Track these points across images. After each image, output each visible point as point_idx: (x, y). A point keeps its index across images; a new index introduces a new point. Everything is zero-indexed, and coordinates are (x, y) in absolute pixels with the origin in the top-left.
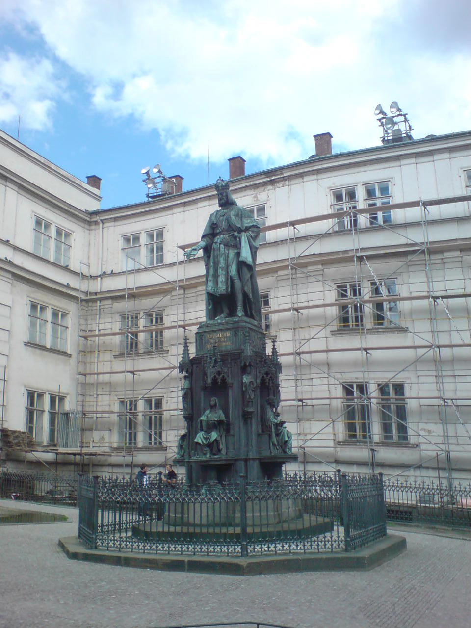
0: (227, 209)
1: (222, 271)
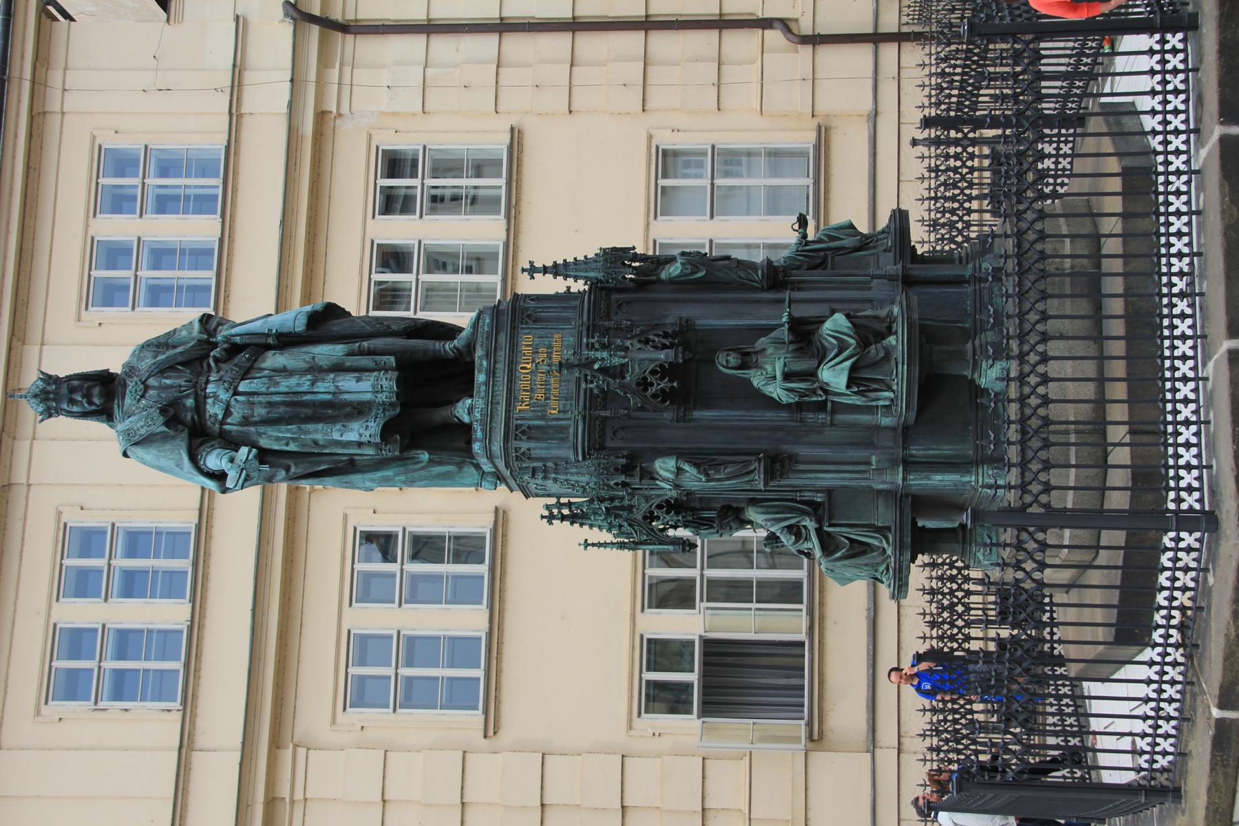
0: (125, 386)
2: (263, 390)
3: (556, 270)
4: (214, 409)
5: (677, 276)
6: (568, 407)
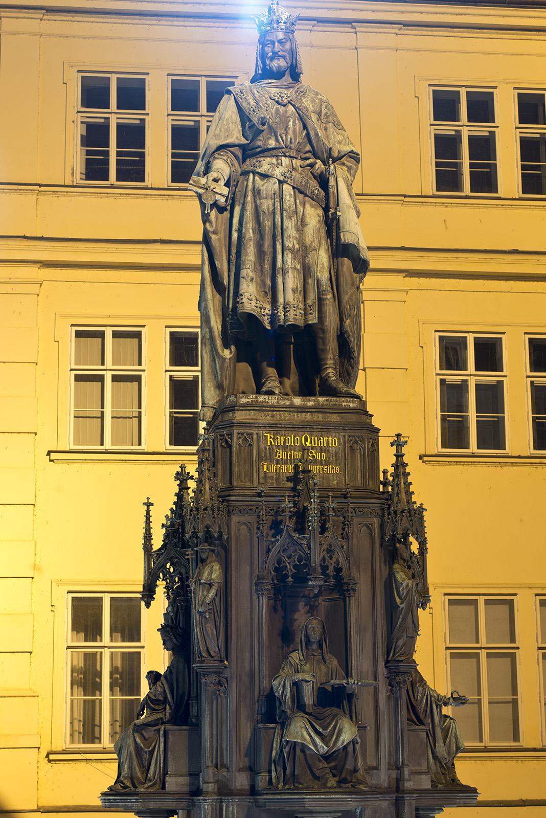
1: (294, 258)
2: (285, 206)
3: (400, 465)
4: (265, 165)
5: (396, 580)
6: (270, 481)
